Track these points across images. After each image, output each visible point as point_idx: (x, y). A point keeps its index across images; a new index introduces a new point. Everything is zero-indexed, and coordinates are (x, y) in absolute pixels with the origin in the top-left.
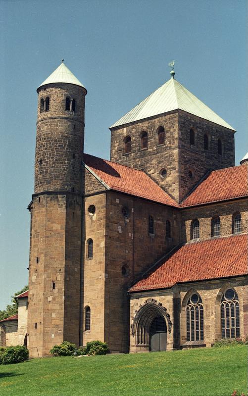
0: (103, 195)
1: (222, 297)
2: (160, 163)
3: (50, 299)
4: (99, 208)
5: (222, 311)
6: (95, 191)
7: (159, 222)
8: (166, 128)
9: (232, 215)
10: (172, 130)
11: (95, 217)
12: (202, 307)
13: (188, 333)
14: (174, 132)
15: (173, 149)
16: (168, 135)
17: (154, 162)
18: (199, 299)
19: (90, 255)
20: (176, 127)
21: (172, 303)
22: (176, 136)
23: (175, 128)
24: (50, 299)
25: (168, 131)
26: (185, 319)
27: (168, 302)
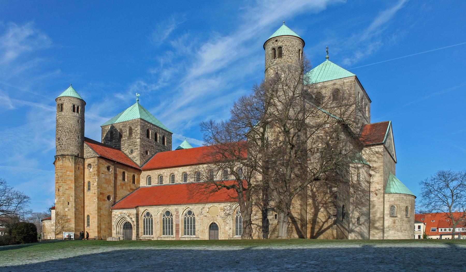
1: (163, 214)
3: (66, 210)
5: (164, 221)
8: (133, 128)
10: (136, 129)
12: (152, 219)
13: (144, 231)
14: (138, 130)
16: (134, 131)
19: (89, 189)
20: (139, 127)
22: (139, 132)
23: (138, 128)
24: (66, 210)
25: (134, 129)
26: (143, 225)
27: (133, 215)
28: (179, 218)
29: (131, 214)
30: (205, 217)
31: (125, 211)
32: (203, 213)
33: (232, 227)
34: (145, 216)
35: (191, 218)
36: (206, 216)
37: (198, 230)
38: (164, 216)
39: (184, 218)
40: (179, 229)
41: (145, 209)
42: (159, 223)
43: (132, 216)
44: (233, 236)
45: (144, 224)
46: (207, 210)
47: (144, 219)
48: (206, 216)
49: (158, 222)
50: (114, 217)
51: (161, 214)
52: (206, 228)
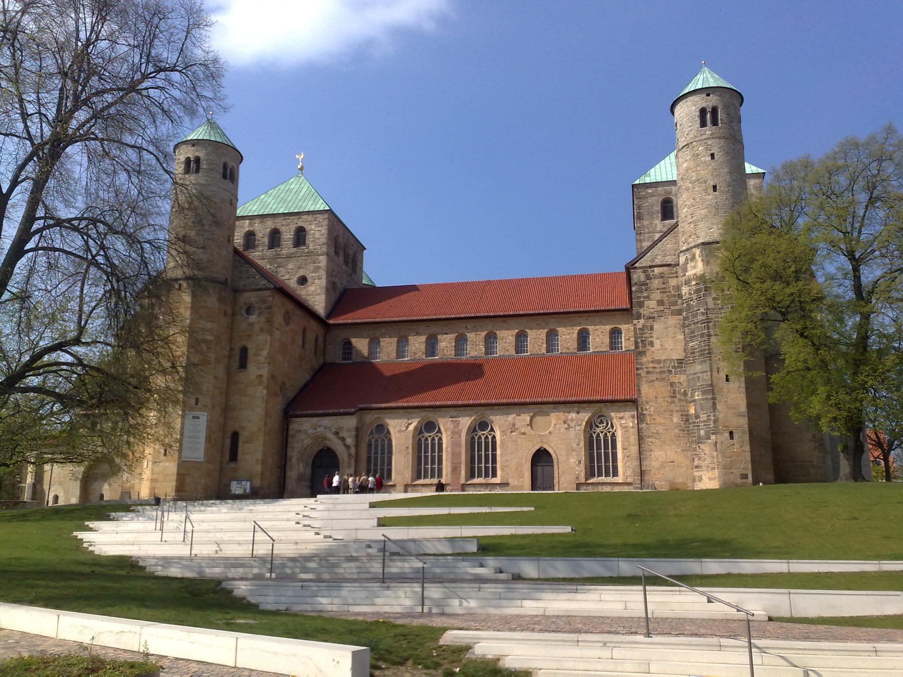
0: (268, 293)
2: (300, 268)
4: (259, 308)
5: (419, 445)
6: (254, 287)
7: (311, 336)
9: (396, 339)
11: (253, 318)
15: (320, 255)
17: (290, 266)
18: (386, 430)
19: (243, 364)
21: (354, 433)
27: (349, 430)
28: (460, 437)
29: (341, 428)
30: (523, 436)
31: (326, 421)
32: (516, 426)
33: (583, 459)
34: (372, 433)
35: (487, 438)
36: (524, 434)
37: (507, 467)
38: (421, 432)
39: (470, 437)
40: (461, 463)
41: (376, 416)
42: (410, 451)
43: (344, 434)
44: (587, 479)
45: (369, 452)
46: (525, 420)
47: (370, 440)
48: (524, 434)
49: (407, 447)
50: (293, 436)
51: (416, 428)
52: (524, 460)
